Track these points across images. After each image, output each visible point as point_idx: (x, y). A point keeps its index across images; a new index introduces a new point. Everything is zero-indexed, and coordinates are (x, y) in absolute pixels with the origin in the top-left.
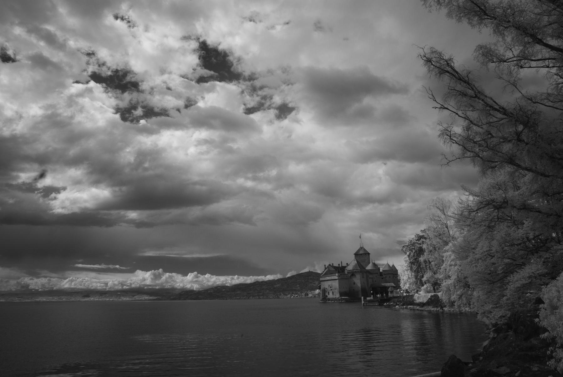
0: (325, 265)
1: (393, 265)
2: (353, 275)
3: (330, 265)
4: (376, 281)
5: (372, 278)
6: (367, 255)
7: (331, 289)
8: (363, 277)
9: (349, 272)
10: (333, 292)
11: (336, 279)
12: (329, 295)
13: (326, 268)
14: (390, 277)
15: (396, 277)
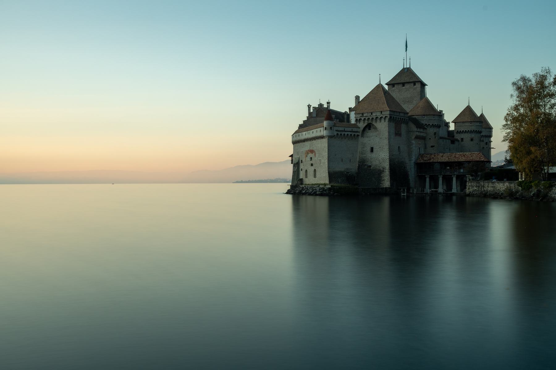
0: (309, 106)
1: (482, 115)
2: (370, 129)
3: (321, 105)
4: (432, 147)
5: (424, 138)
6: (418, 85)
7: (311, 162)
8: (398, 134)
9: (360, 119)
10: (315, 170)
11: (322, 137)
12: (306, 177)
13: (310, 113)
14: (472, 140)
15: (486, 143)
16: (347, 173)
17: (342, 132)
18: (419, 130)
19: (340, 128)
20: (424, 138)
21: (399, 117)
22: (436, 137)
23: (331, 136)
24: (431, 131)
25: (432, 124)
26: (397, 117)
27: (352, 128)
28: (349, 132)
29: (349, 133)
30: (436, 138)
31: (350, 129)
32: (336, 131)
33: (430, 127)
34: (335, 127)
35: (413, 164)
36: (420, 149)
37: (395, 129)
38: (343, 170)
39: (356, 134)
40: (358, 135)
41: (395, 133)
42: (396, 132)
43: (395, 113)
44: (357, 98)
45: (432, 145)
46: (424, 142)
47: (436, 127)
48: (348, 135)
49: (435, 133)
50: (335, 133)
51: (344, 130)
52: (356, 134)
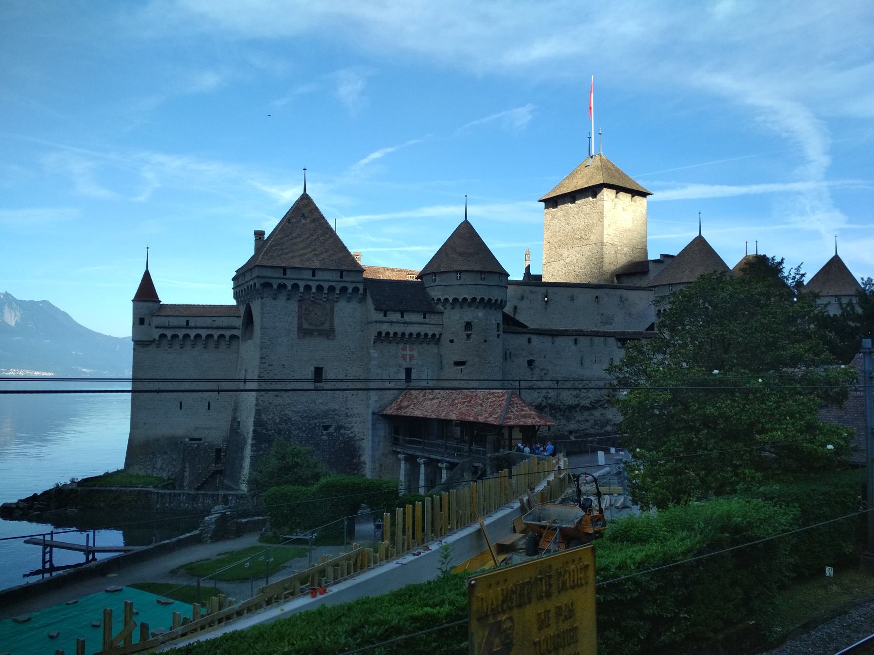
4: (458, 364)
5: (435, 339)
16: (192, 439)
17: (177, 330)
18: (395, 316)
19: (171, 319)
20: (435, 339)
21: (310, 283)
22: (472, 336)
23: (140, 341)
24: (454, 319)
25: (455, 300)
26: (302, 285)
27: (214, 319)
28: (204, 330)
29: (204, 333)
30: (472, 340)
31: (208, 322)
32: (157, 327)
33: (453, 308)
34: (154, 318)
35: (370, 418)
36: (413, 370)
37: (300, 318)
38: (179, 432)
39: (228, 333)
40: (233, 337)
41: (300, 329)
42: (306, 326)
43: (288, 272)
44: (259, 234)
45: (457, 358)
46: (436, 351)
47: (469, 306)
48: (198, 336)
49: (468, 326)
50: (156, 334)
51: (184, 323)
52: (228, 333)
